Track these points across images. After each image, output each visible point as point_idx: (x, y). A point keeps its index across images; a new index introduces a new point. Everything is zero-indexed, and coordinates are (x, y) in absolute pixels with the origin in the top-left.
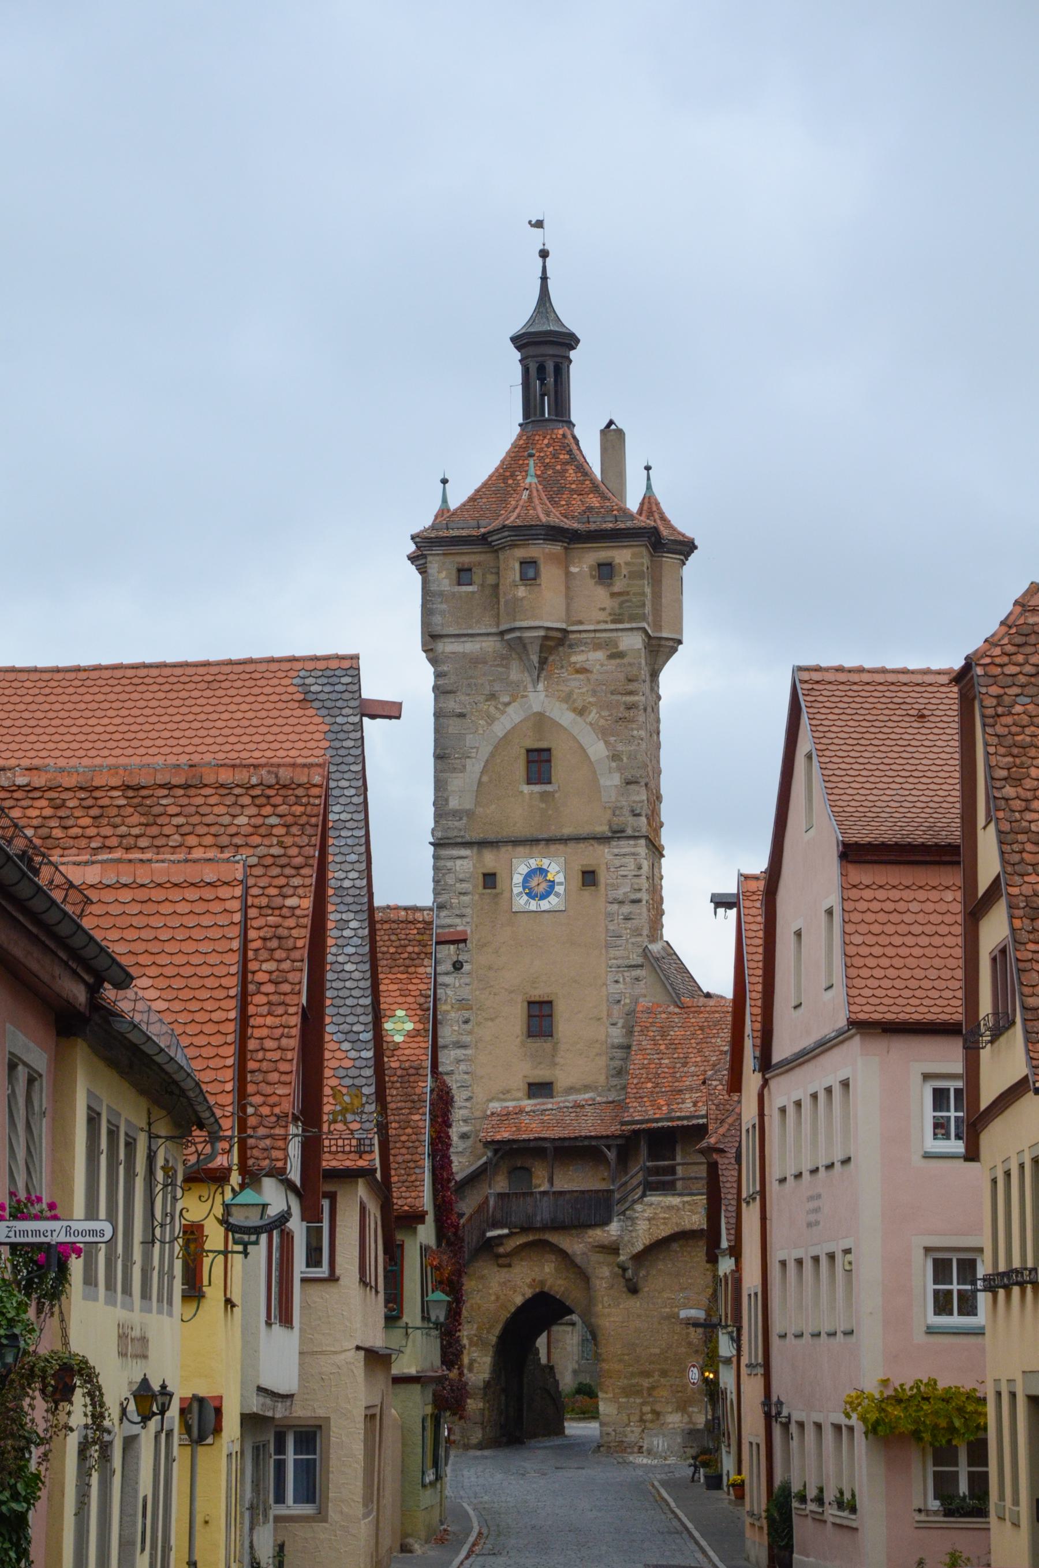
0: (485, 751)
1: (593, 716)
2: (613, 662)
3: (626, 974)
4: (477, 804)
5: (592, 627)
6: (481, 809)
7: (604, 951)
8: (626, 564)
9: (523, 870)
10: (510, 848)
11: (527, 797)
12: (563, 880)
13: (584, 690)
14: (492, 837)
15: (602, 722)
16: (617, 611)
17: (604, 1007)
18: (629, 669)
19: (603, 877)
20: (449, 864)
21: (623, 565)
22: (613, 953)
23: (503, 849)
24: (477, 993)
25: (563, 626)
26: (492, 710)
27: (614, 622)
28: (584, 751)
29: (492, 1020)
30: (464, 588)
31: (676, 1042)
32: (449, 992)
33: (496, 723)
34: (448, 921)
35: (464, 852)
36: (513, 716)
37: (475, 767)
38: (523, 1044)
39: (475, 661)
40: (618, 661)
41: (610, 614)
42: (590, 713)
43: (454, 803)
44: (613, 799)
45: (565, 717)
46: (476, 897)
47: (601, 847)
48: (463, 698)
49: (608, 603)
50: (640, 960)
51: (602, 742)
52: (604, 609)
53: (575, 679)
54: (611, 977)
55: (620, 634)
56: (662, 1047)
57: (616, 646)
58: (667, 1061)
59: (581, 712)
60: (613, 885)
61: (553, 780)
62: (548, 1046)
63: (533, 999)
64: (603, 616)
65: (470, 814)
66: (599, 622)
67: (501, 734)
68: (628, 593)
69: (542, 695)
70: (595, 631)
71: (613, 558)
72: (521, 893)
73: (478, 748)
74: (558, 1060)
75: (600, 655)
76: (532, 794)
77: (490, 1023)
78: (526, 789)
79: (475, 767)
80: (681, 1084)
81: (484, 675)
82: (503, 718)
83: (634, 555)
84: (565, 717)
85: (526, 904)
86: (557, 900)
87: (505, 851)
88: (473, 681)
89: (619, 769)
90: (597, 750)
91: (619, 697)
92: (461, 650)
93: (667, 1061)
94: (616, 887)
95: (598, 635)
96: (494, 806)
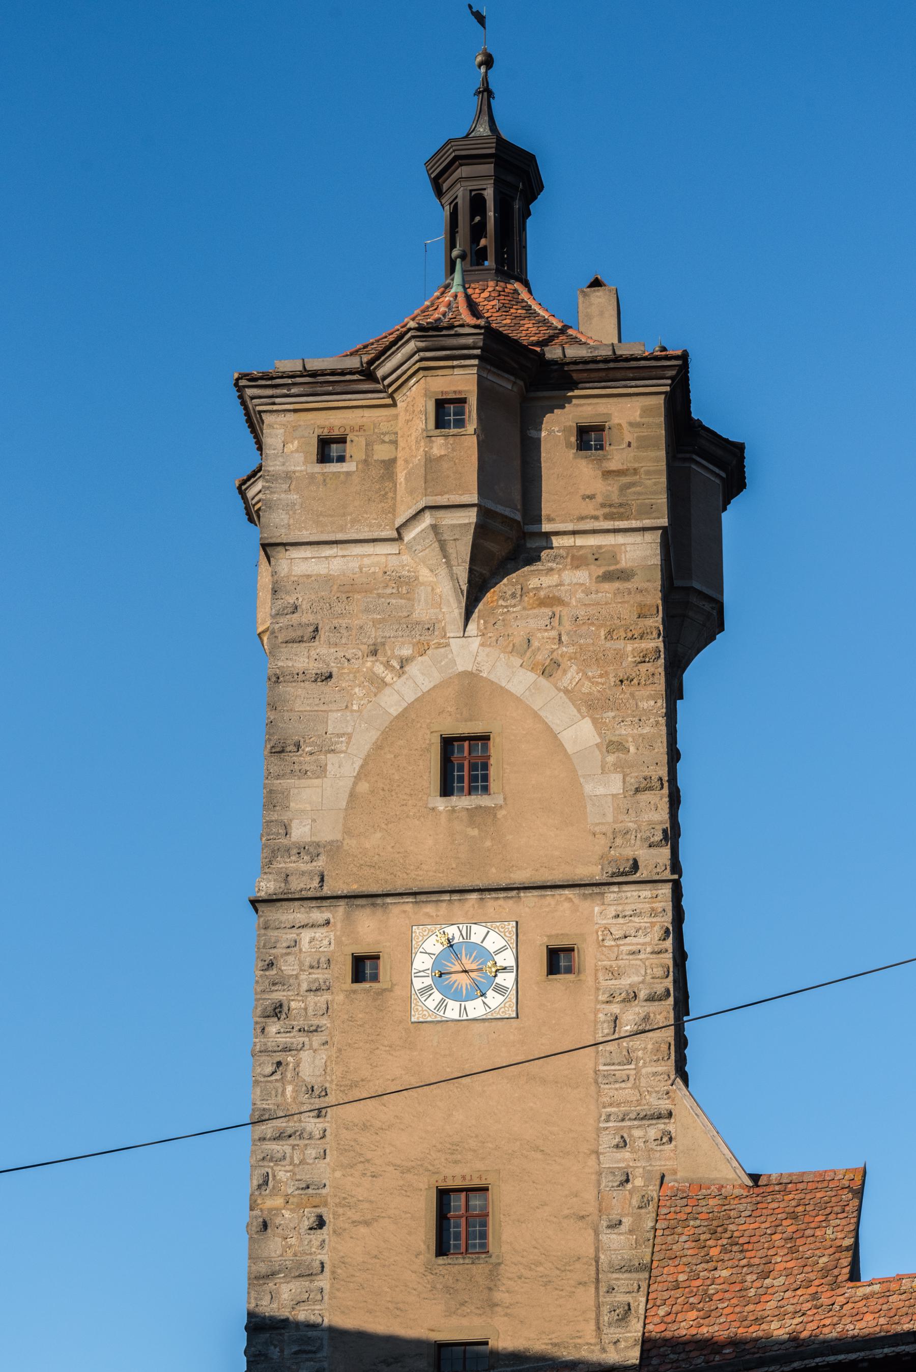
0: (365, 740)
1: (571, 676)
2: (606, 586)
3: (637, 1133)
4: (347, 832)
5: (570, 527)
6: (353, 842)
7: (593, 1088)
8: (631, 424)
9: (434, 945)
10: (408, 908)
11: (443, 819)
12: (513, 964)
13: (554, 633)
14: (374, 889)
15: (586, 687)
16: (615, 498)
17: (590, 1195)
18: (639, 598)
19: (590, 957)
20: (292, 935)
21: (625, 425)
22: (609, 1091)
23: (396, 910)
24: (338, 1174)
25: (518, 517)
26: (379, 669)
27: (607, 517)
28: (555, 736)
29: (367, 1223)
30: (333, 468)
31: (742, 1241)
32: (282, 1175)
33: (387, 691)
34: (283, 1039)
35: (318, 916)
36: (422, 676)
37: (343, 769)
38: (429, 1269)
39: (349, 588)
40: (617, 585)
41: (603, 505)
42: (565, 672)
43: (300, 832)
44: (610, 818)
45: (518, 680)
46: (340, 998)
47: (586, 904)
48: (323, 650)
49: (599, 487)
50: (664, 1105)
51: (588, 720)
52: (591, 497)
53: (536, 616)
54: (608, 1140)
55: (620, 539)
56: (714, 1252)
57: (614, 558)
58: (725, 1273)
59: (549, 669)
60: (609, 970)
61: (493, 785)
62: (479, 1270)
63: (450, 1184)
64: (589, 508)
65: (333, 849)
66: (582, 518)
67: (394, 711)
68: (636, 471)
69: (475, 643)
70: (574, 533)
71: (609, 415)
72: (429, 988)
73: (350, 736)
74: (498, 1296)
75: (582, 576)
76: (453, 810)
77: (363, 1230)
78: (441, 804)
79: (343, 769)
80: (759, 1307)
81: (367, 610)
82: (399, 683)
83: (645, 411)
84: (518, 680)
85: (438, 1008)
86: (500, 998)
87: (400, 913)
88: (344, 622)
89: (619, 767)
90: (580, 734)
91: (620, 644)
92: (323, 571)
93: (725, 1273)
94: (615, 974)
95: (580, 541)
96: (378, 835)
